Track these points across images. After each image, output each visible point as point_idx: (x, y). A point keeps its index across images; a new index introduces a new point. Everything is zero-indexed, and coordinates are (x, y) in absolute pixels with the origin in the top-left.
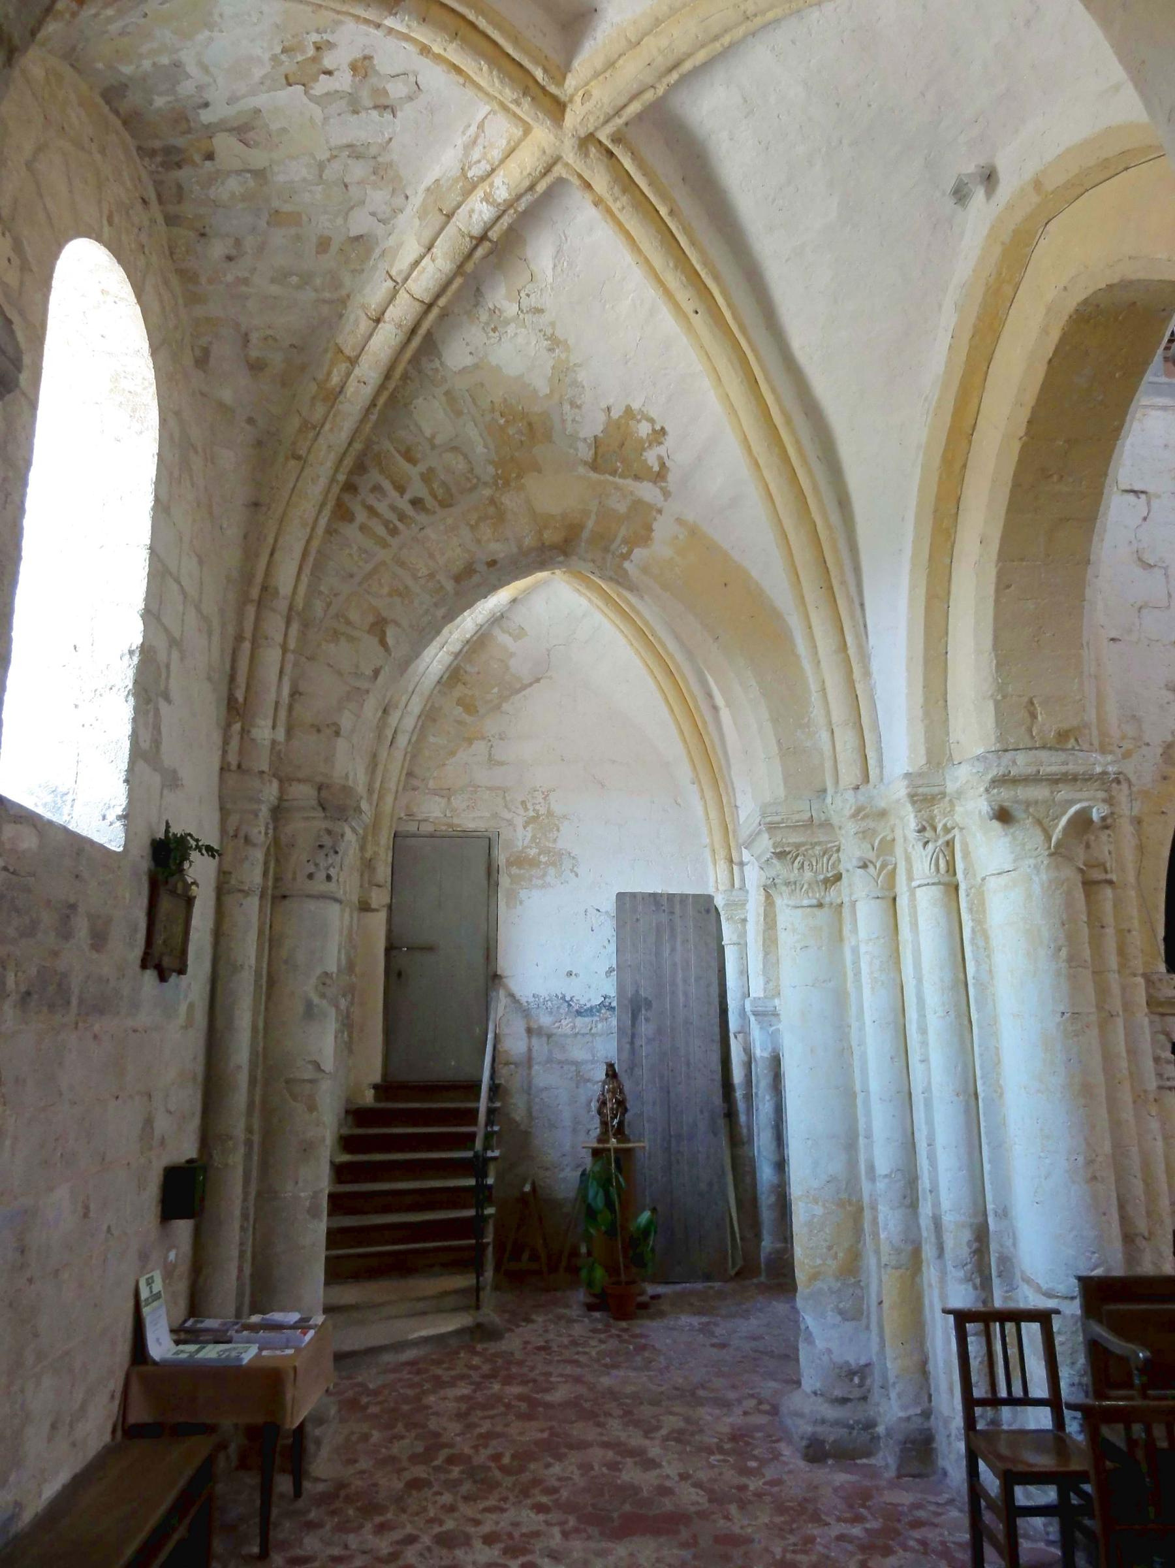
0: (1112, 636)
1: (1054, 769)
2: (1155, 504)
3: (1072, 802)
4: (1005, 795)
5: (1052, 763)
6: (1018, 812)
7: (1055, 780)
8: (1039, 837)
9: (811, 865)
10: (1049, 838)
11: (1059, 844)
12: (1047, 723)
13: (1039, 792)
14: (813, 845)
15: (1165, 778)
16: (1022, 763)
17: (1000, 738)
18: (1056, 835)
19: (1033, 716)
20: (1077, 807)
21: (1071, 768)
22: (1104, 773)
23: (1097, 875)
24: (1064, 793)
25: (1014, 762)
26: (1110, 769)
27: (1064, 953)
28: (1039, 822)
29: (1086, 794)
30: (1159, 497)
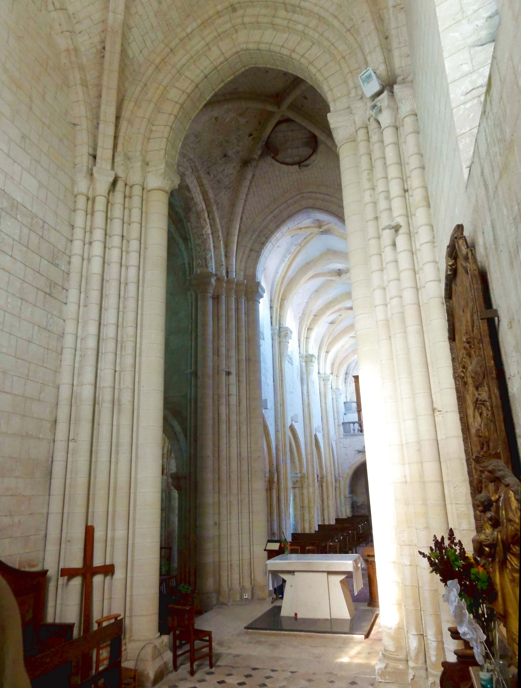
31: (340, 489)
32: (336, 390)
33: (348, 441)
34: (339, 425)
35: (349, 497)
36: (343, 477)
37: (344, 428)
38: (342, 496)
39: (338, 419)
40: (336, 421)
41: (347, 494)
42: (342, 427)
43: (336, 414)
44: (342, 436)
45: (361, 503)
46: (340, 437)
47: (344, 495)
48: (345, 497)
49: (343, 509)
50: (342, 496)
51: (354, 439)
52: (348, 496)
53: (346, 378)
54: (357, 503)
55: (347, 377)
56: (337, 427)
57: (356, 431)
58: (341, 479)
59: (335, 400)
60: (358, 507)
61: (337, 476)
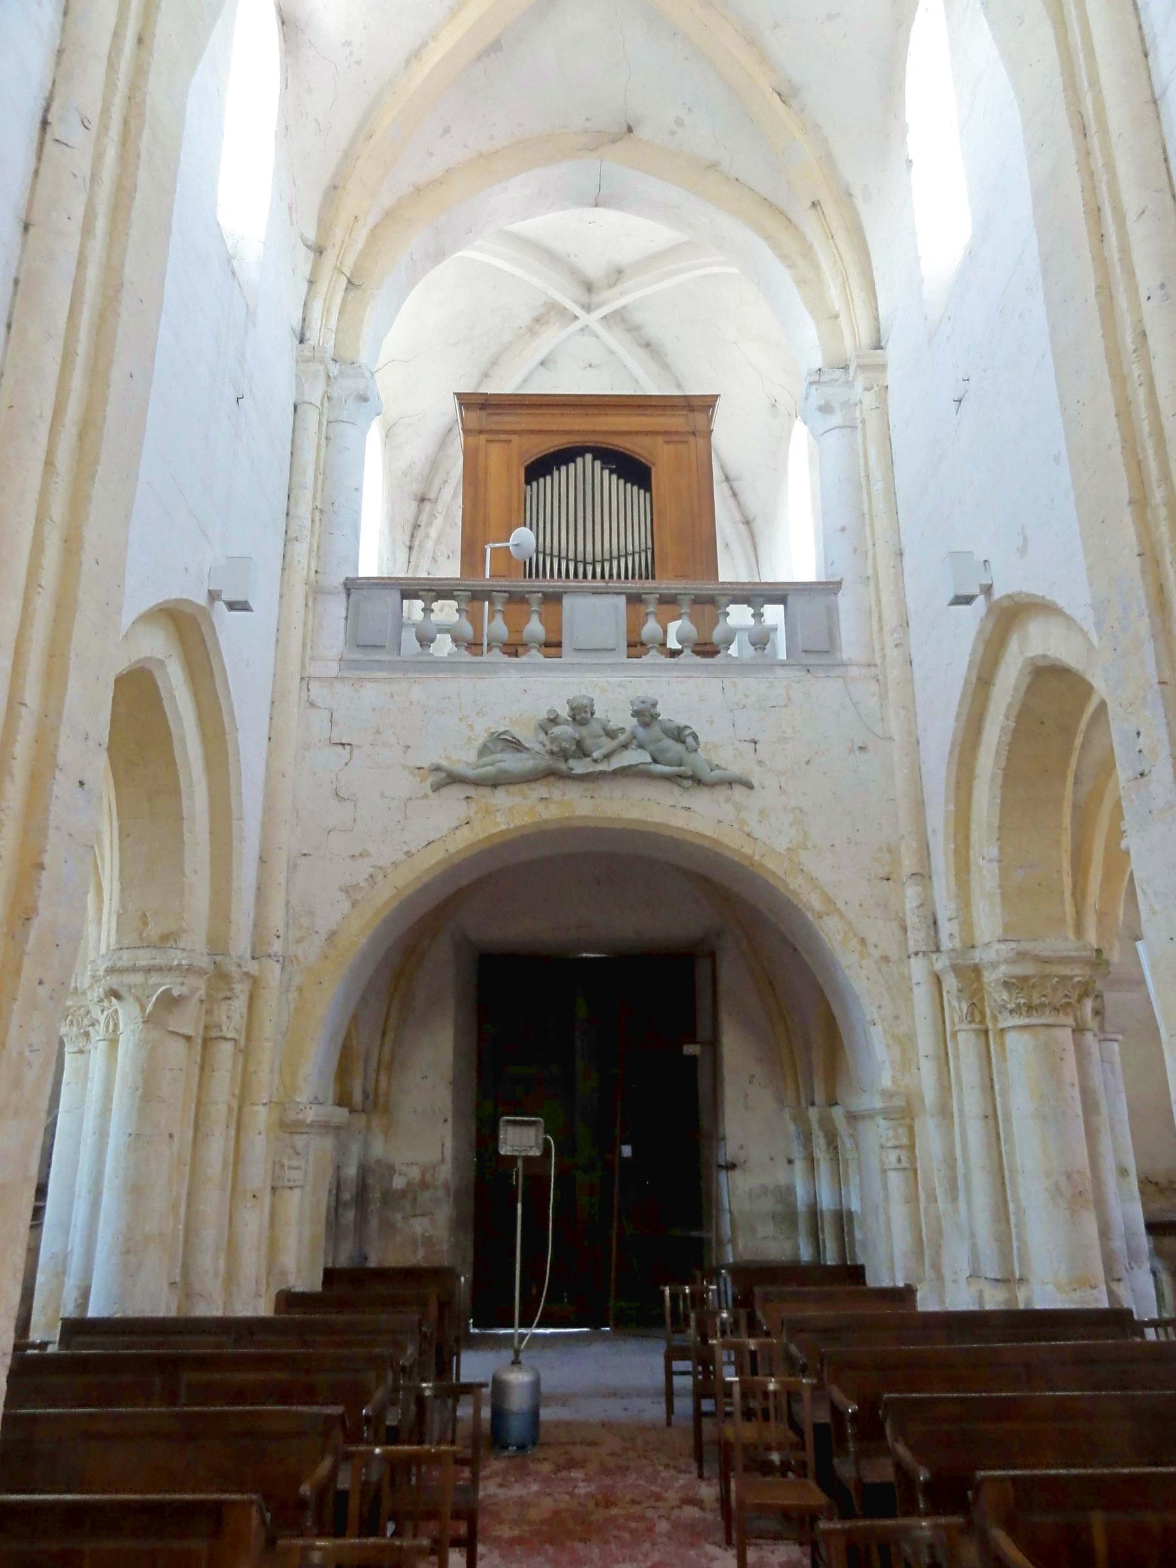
0: (305, 852)
1: (143, 963)
2: (356, 752)
3: (160, 985)
4: (114, 981)
5: (144, 958)
6: (123, 992)
7: (149, 970)
8: (136, 1010)
9: (78, 1023)
10: (143, 1007)
11: (150, 1015)
12: (153, 931)
13: (138, 978)
14: (80, 1008)
15: (326, 957)
16: (126, 959)
17: (118, 941)
18: (149, 1008)
19: (145, 924)
20: (163, 988)
21: (158, 961)
22: (179, 965)
23: (214, 1033)
24: (154, 979)
25: (120, 958)
26: (184, 962)
27: (139, 1092)
28: (138, 1000)
29: (168, 980)
30: (359, 747)
31: (245, 1053)
32: (334, 369)
33: (373, 693)
34: (316, 592)
35: (325, 1127)
36: (286, 961)
37: (353, 617)
38: (261, 1117)
39: (319, 551)
40: (300, 550)
41: (303, 1098)
42: (337, 608)
43: (304, 509)
44: (333, 669)
45: (415, 1173)
46: (313, 670)
47: (280, 1105)
48: (288, 1127)
49: (252, 1222)
50: (261, 1117)
51: (417, 693)
52: (310, 1115)
53: (416, 526)
54: (391, 1169)
55: (424, 517)
56: (299, 592)
57: (444, 646)
58: (273, 973)
59: (311, 419)
60: (390, 1199)
61: (241, 943)
